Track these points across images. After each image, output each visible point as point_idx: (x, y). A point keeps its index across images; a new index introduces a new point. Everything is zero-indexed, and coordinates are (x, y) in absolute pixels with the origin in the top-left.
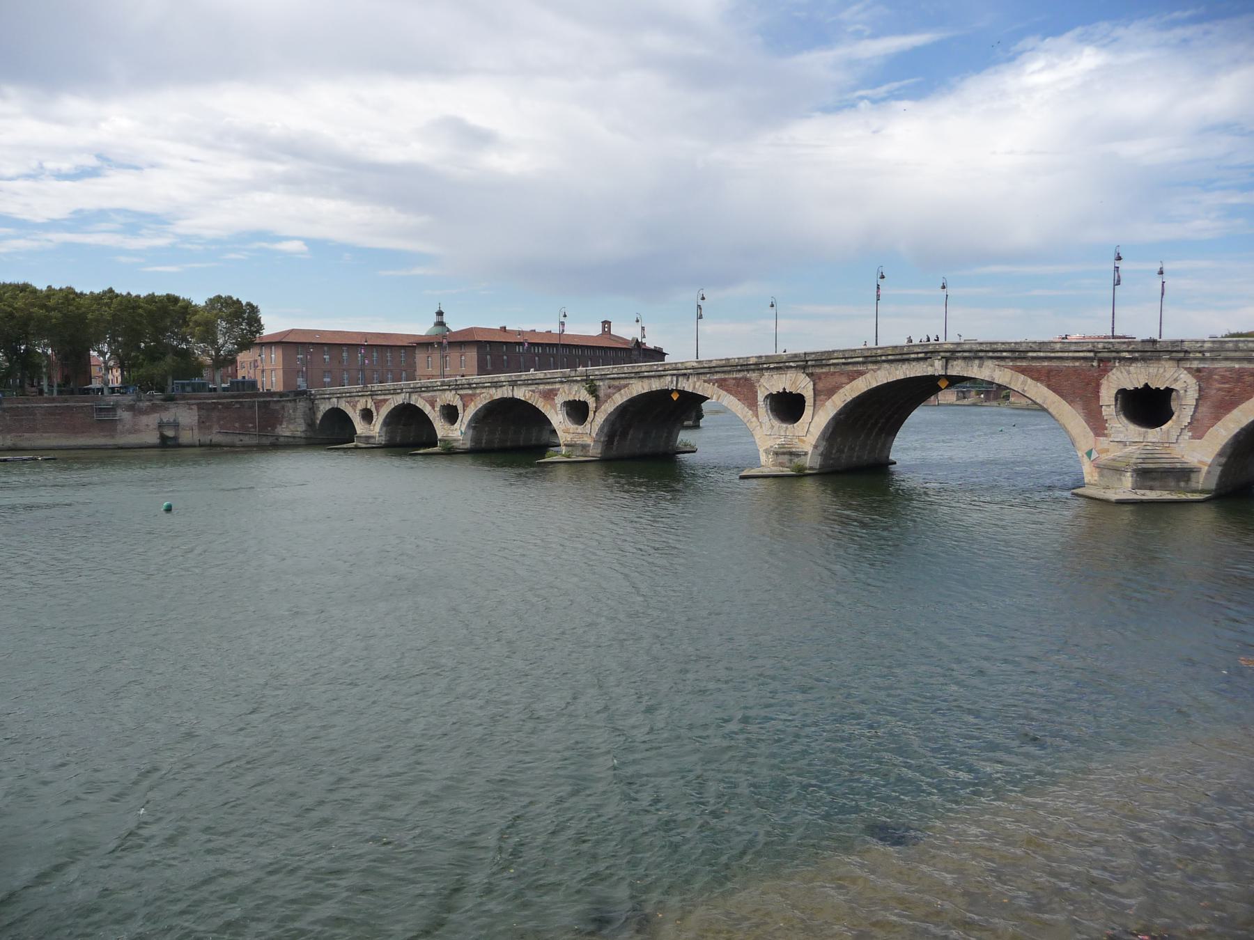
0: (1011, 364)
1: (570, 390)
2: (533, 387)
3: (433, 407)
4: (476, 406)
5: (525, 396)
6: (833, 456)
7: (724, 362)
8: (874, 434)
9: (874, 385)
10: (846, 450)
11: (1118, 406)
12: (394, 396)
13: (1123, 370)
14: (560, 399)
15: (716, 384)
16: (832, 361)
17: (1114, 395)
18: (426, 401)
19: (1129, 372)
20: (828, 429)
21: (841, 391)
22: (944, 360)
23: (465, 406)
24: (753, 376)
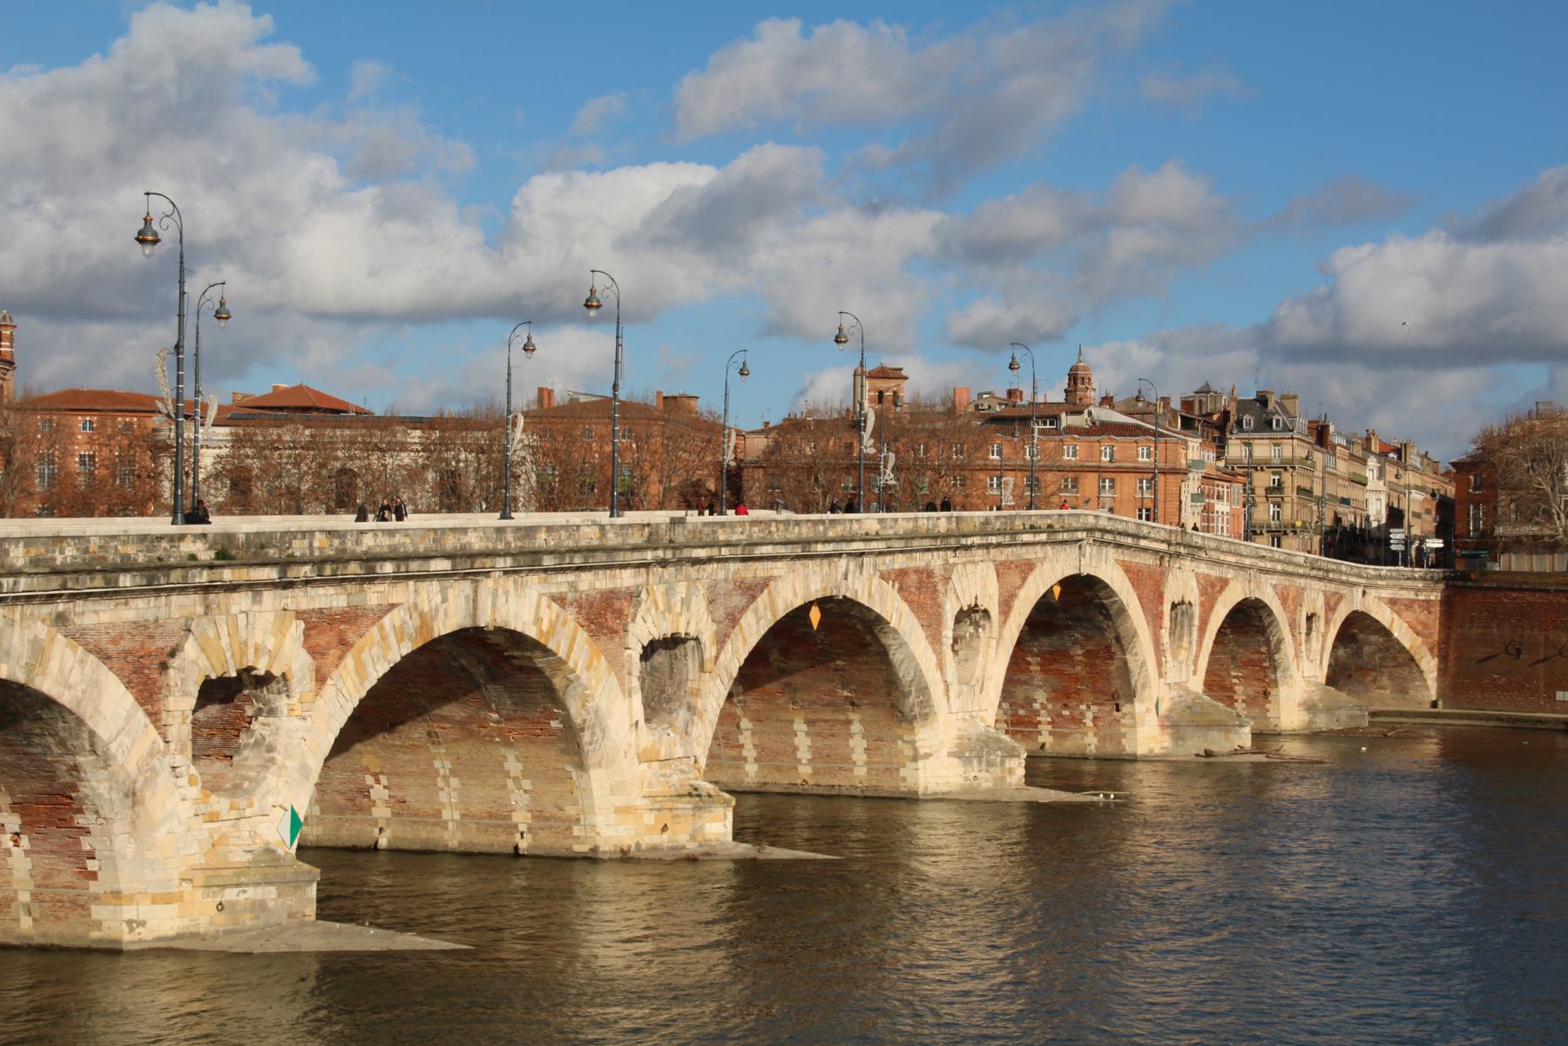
1: (668, 593)
2: (561, 583)
4: (360, 670)
15: (897, 585)
18: (105, 657)
23: (321, 679)
24: (936, 561)
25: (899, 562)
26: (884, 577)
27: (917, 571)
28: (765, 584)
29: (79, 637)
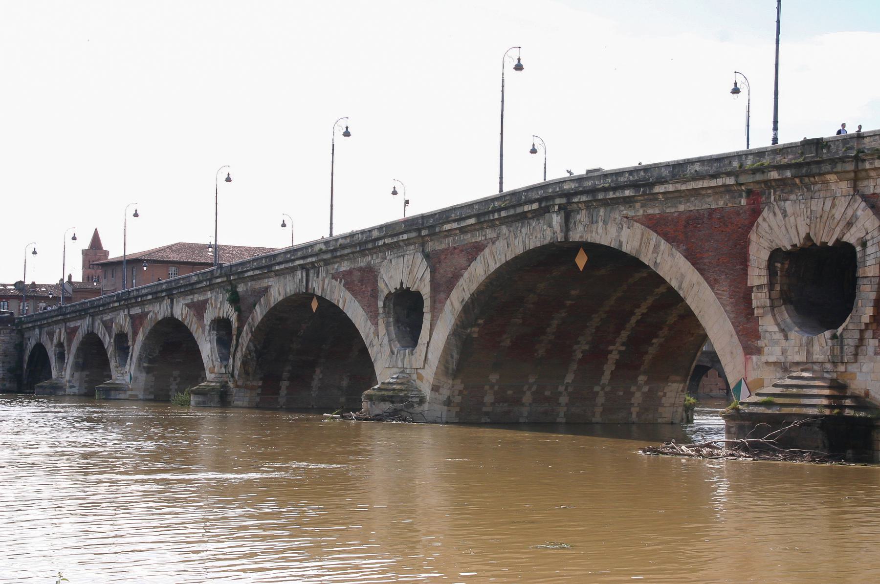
0: (641, 212)
5: (182, 314)
6: (485, 409)
7: (348, 241)
8: (606, 378)
9: (493, 267)
10: (527, 398)
11: (778, 288)
13: (777, 210)
14: (209, 316)
15: (343, 281)
16: (447, 227)
17: (764, 264)
19: (785, 214)
20: (452, 357)
21: (461, 281)
22: (562, 212)
25: (345, 266)
26: (334, 277)
27: (360, 269)
28: (266, 290)
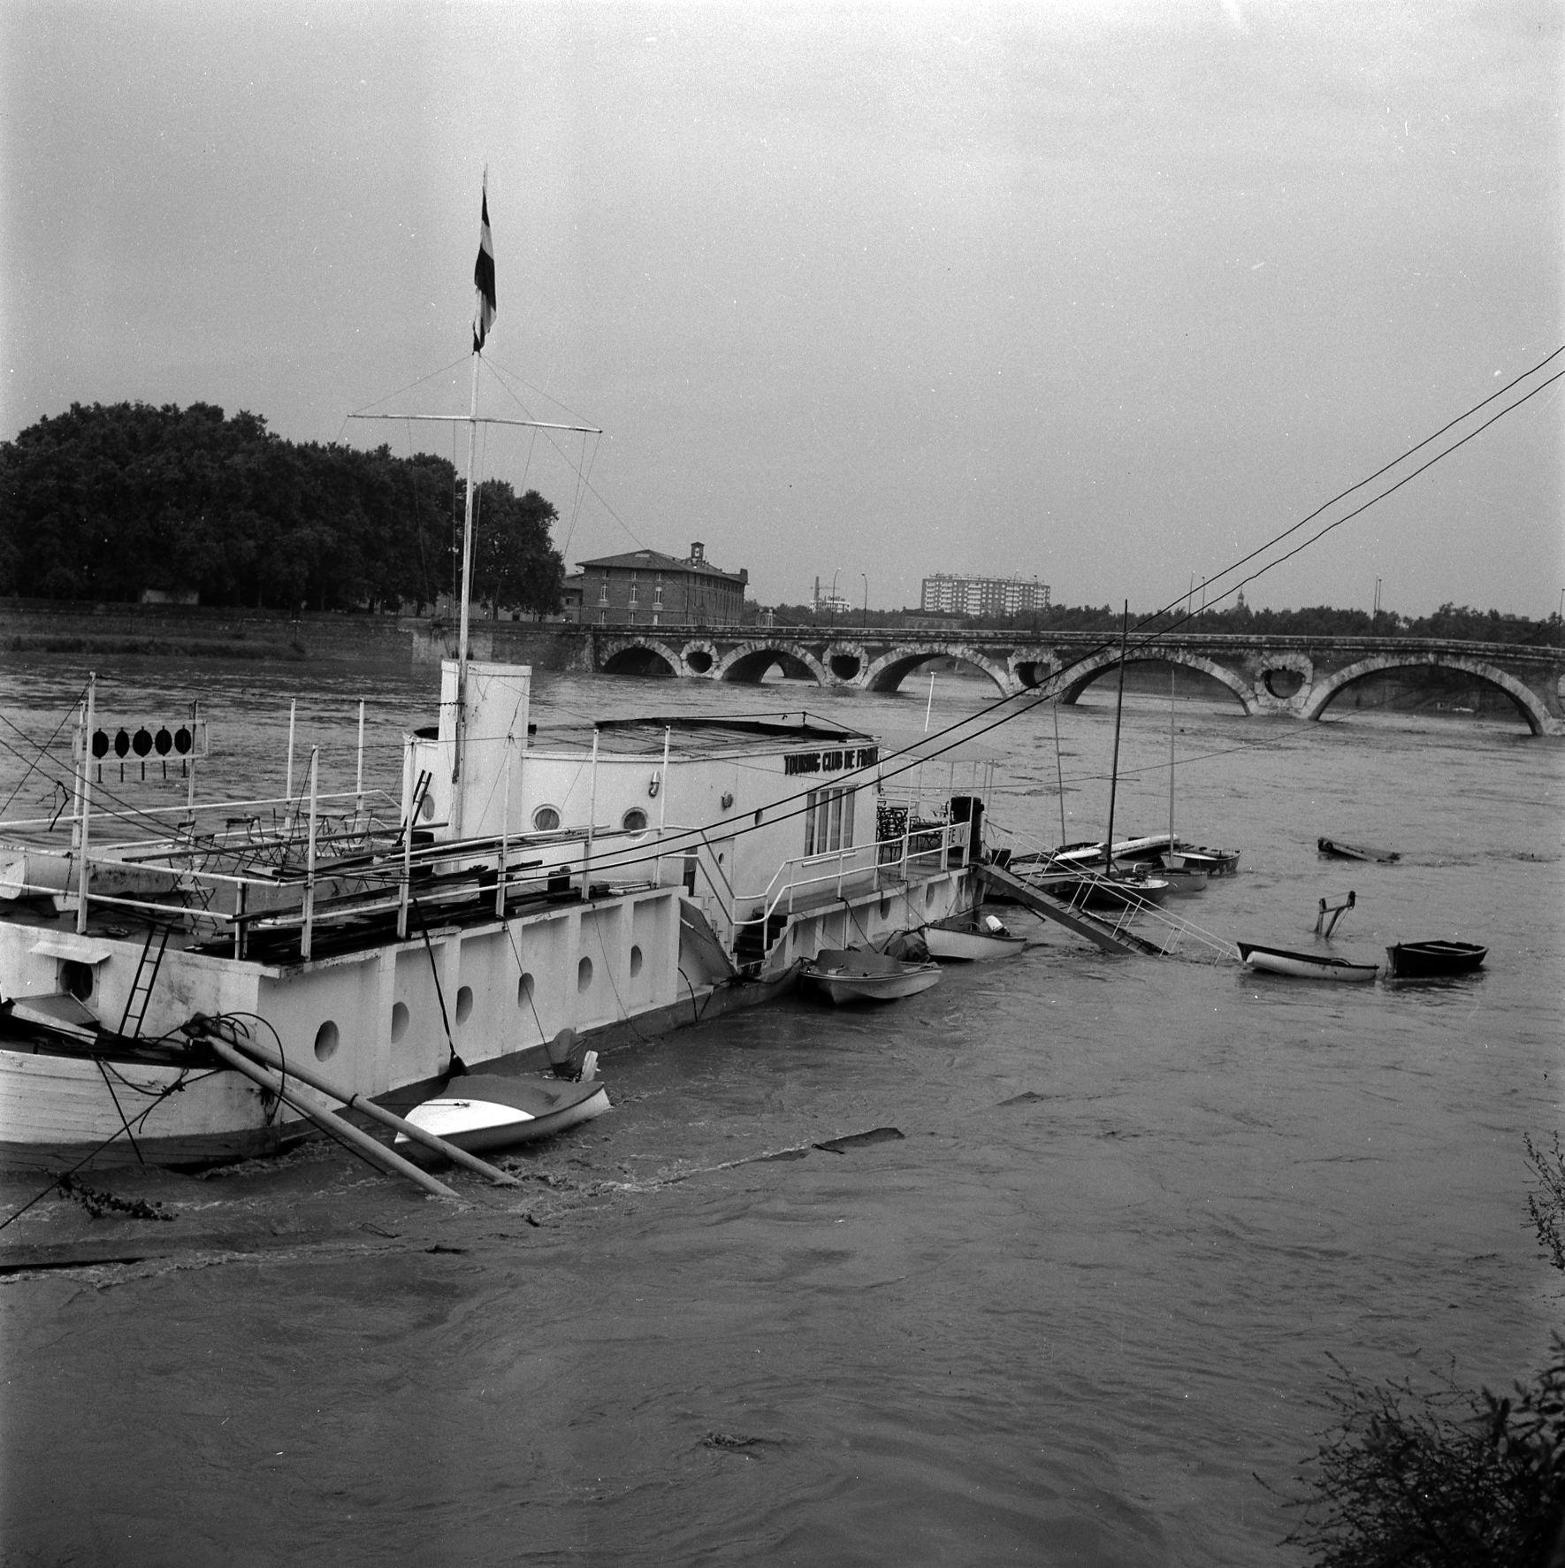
3: (819, 659)
12: (751, 641)
14: (1012, 662)
23: (870, 662)
29: (804, 647)
